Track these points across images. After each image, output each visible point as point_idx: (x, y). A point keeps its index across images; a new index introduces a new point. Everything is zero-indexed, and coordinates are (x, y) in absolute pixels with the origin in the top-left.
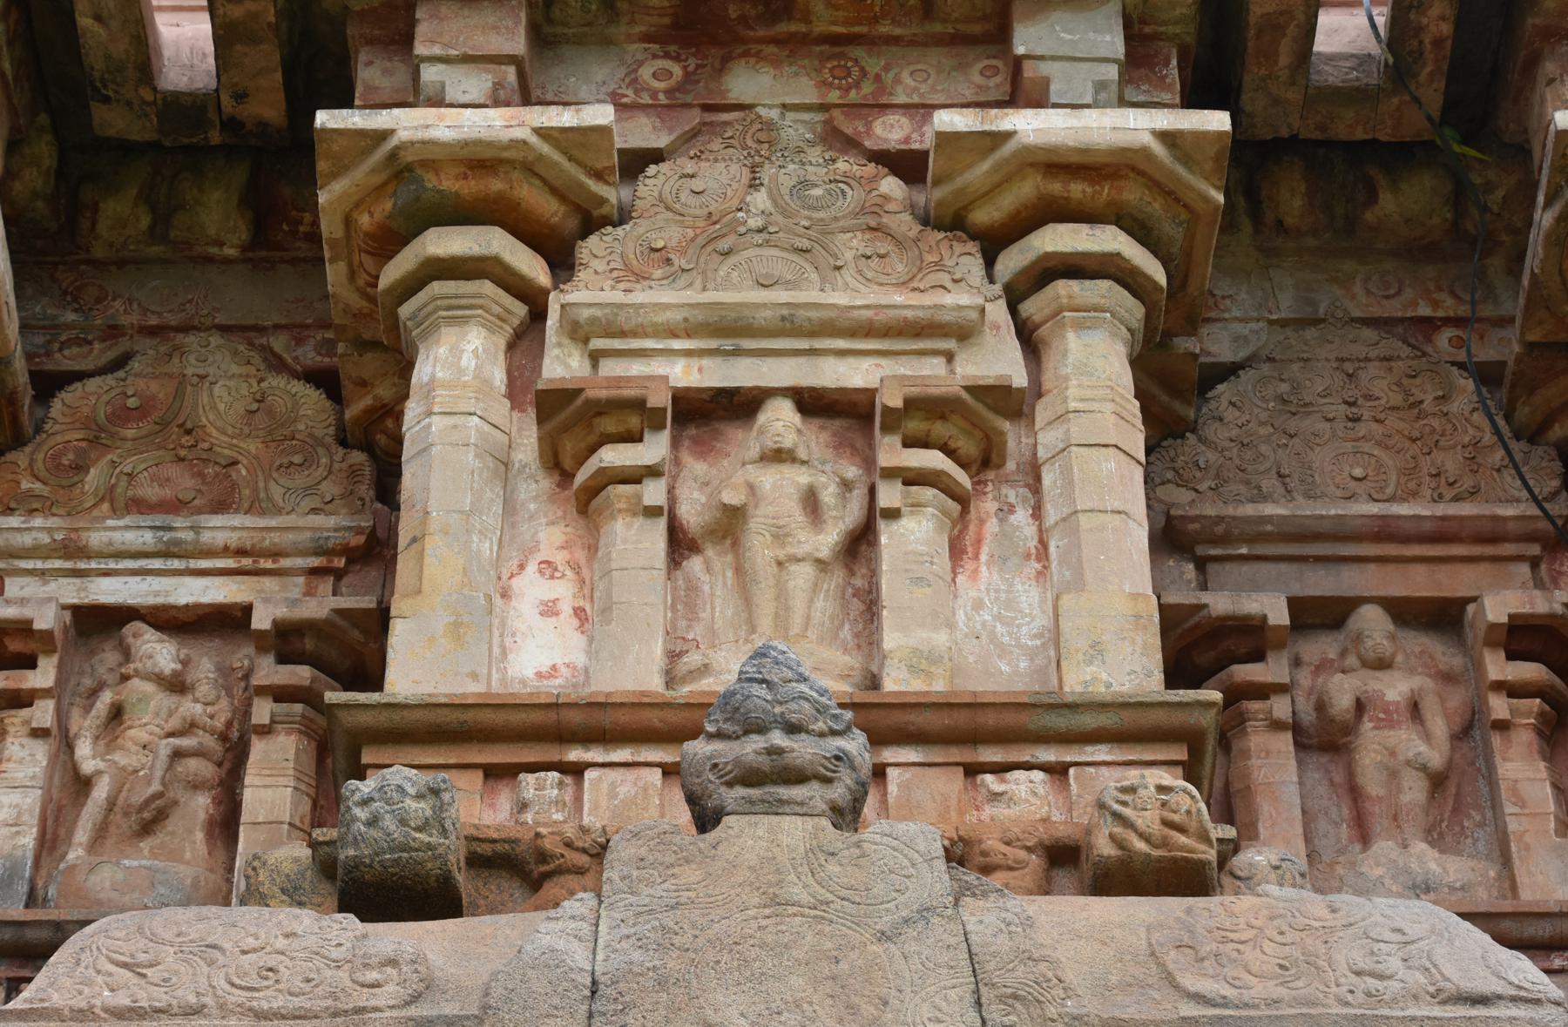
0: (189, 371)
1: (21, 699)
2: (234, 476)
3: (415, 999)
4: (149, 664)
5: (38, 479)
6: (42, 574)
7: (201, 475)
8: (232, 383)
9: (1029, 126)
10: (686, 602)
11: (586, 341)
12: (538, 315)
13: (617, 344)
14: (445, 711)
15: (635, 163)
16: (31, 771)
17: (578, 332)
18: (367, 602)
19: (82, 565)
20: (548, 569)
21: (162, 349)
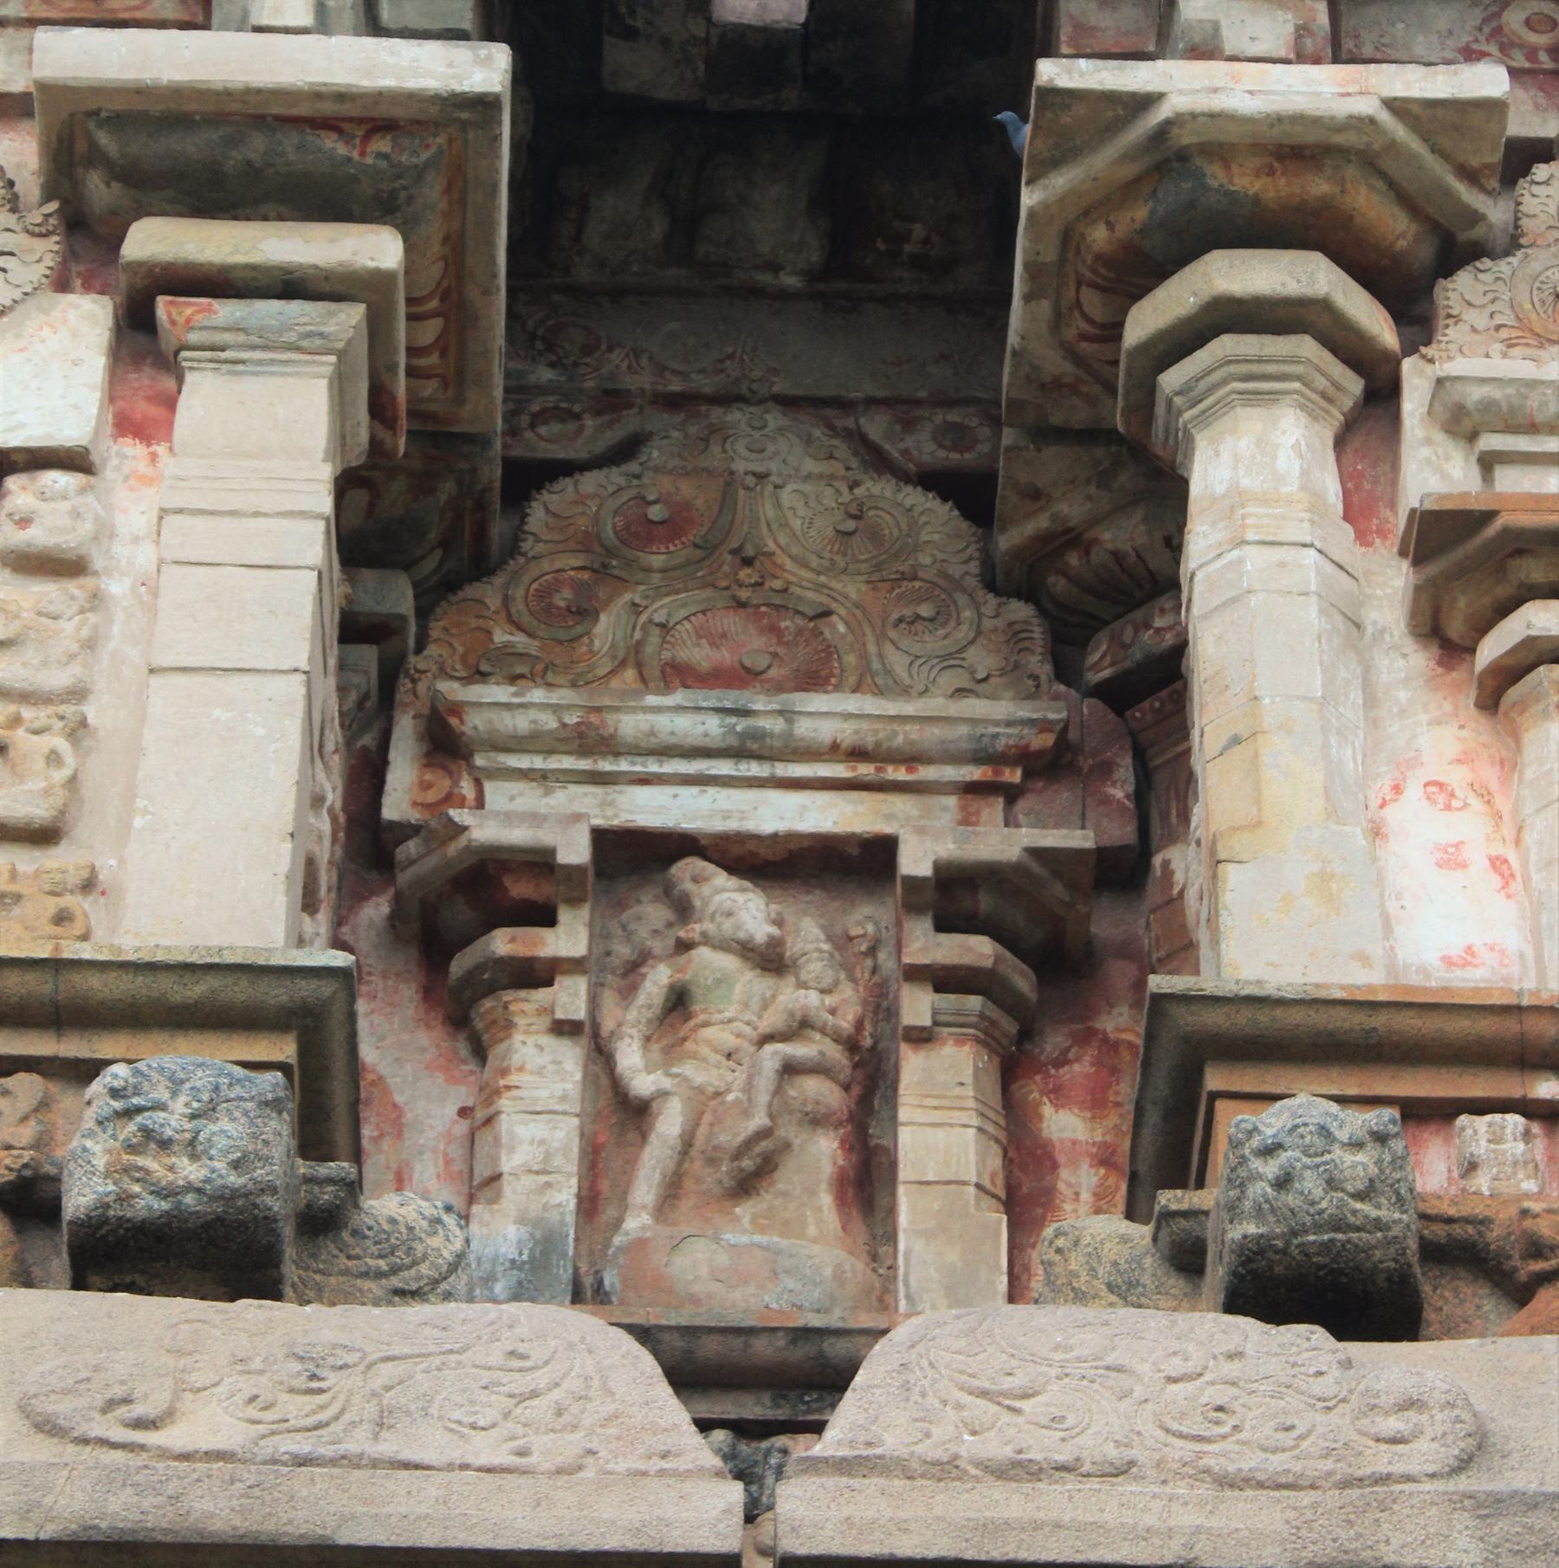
0: (740, 466)
2: (827, 634)
3: (1463, 1465)
4: (727, 926)
5: (520, 628)
6: (542, 777)
7: (774, 629)
8: (807, 488)
11: (1472, 437)
12: (1382, 392)
13: (1523, 443)
14: (1342, 1012)
16: (559, 1088)
17: (1461, 423)
19: (606, 765)
21: (693, 430)
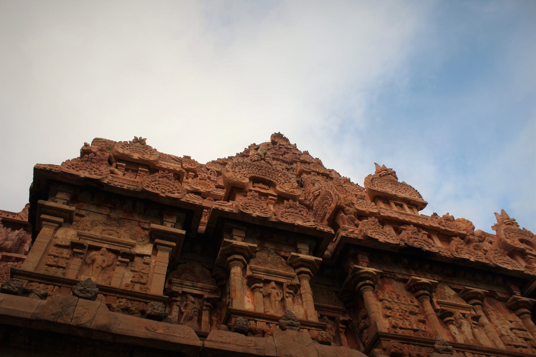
1: (176, 301)
6: (178, 286)
9: (300, 255)
17: (251, 269)
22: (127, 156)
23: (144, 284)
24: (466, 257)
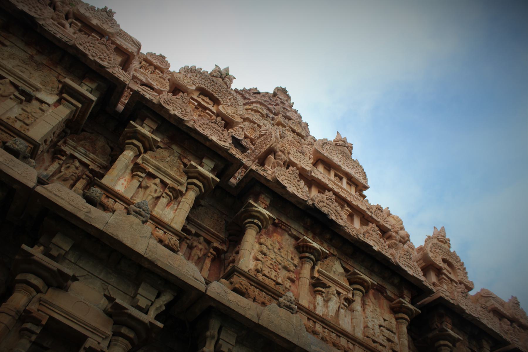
1: (60, 159)
9: (200, 168)
10: (137, 193)
15: (159, 147)
17: (143, 159)
18: (103, 173)
20: (125, 180)
22: (86, 17)
23: (27, 125)
24: (371, 243)
